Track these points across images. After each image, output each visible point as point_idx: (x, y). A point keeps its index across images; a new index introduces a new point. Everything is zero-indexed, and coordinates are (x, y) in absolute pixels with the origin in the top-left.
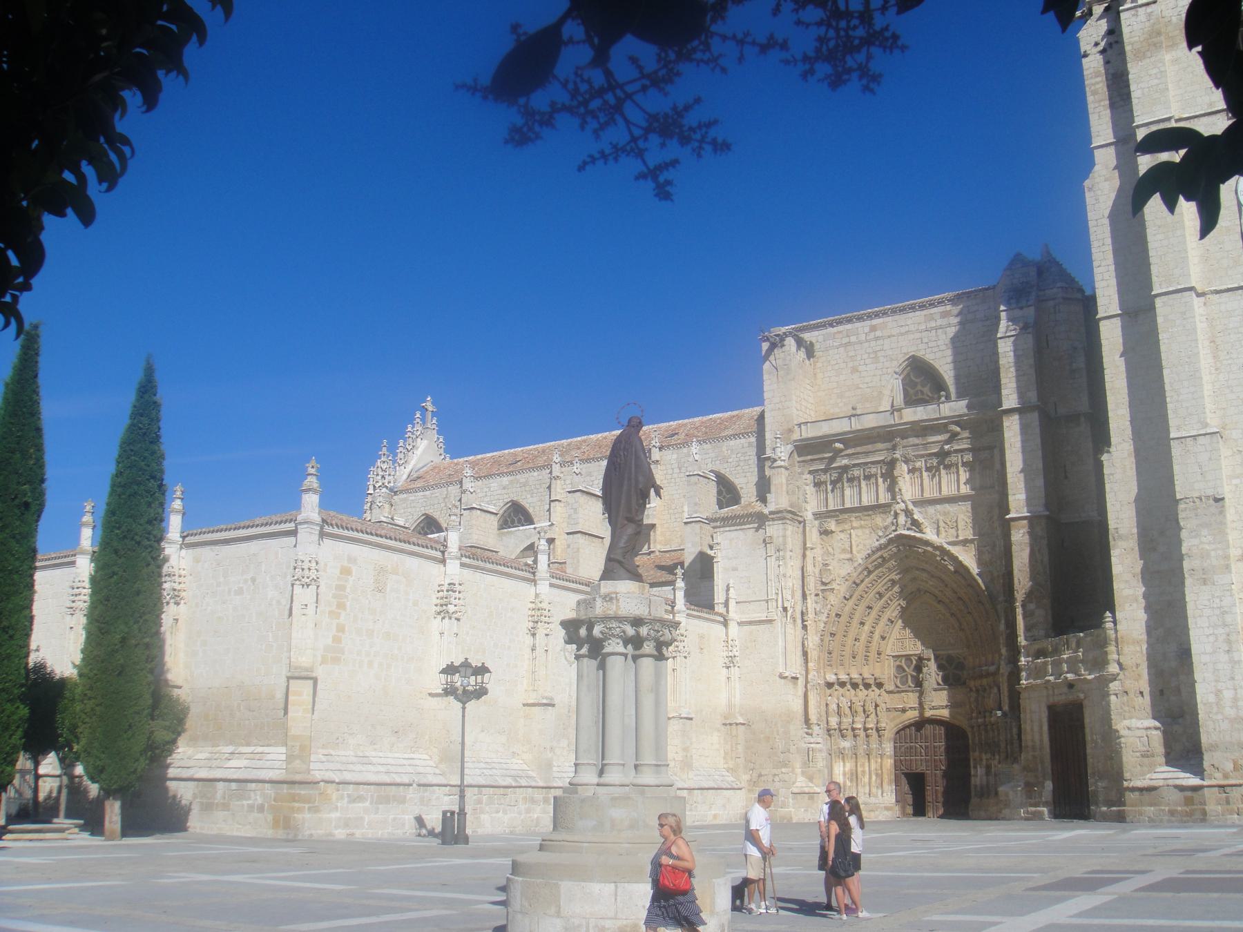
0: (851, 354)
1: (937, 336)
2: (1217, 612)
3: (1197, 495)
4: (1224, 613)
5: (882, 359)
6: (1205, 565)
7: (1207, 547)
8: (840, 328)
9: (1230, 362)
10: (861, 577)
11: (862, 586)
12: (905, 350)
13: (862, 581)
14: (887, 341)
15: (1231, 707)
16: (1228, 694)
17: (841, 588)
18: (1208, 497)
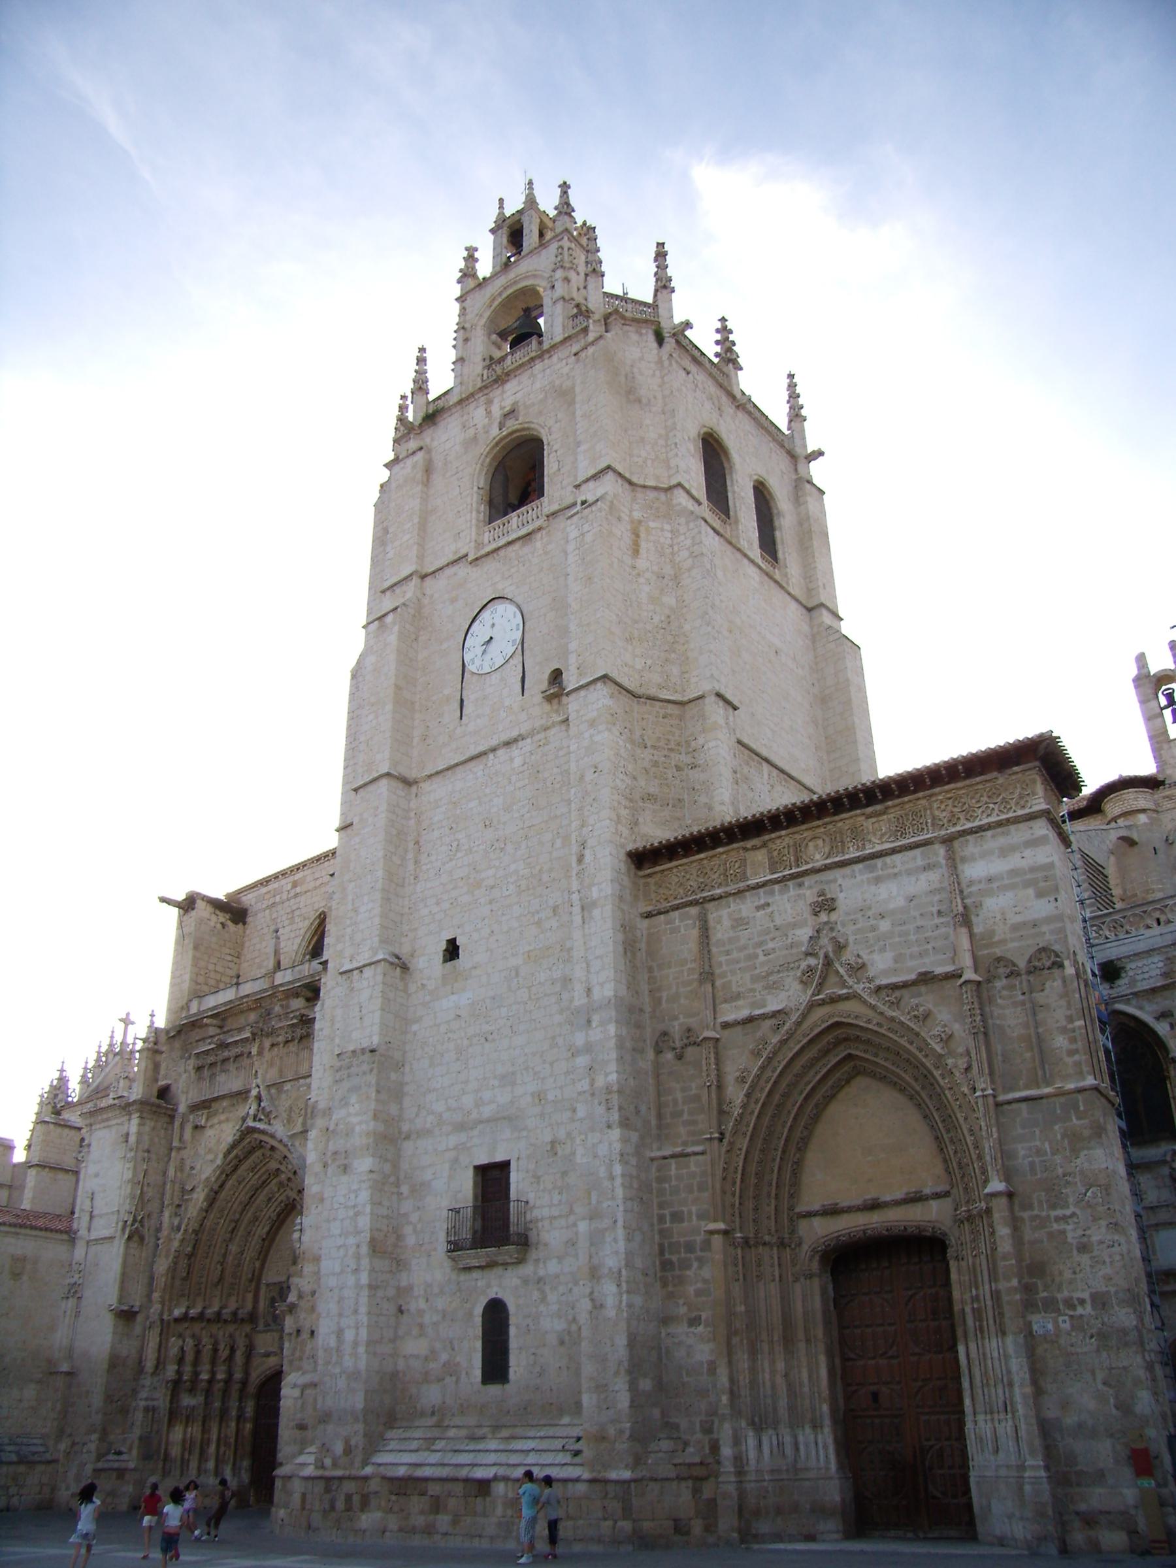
2: (351, 1213)
3: (352, 1048)
5: (297, 919)
7: (354, 1120)
8: (270, 888)
9: (429, 866)
10: (219, 1183)
11: (223, 1195)
12: (316, 906)
13: (222, 1186)
14: (303, 898)
16: (349, 1335)
17: (199, 1197)
18: (363, 1051)
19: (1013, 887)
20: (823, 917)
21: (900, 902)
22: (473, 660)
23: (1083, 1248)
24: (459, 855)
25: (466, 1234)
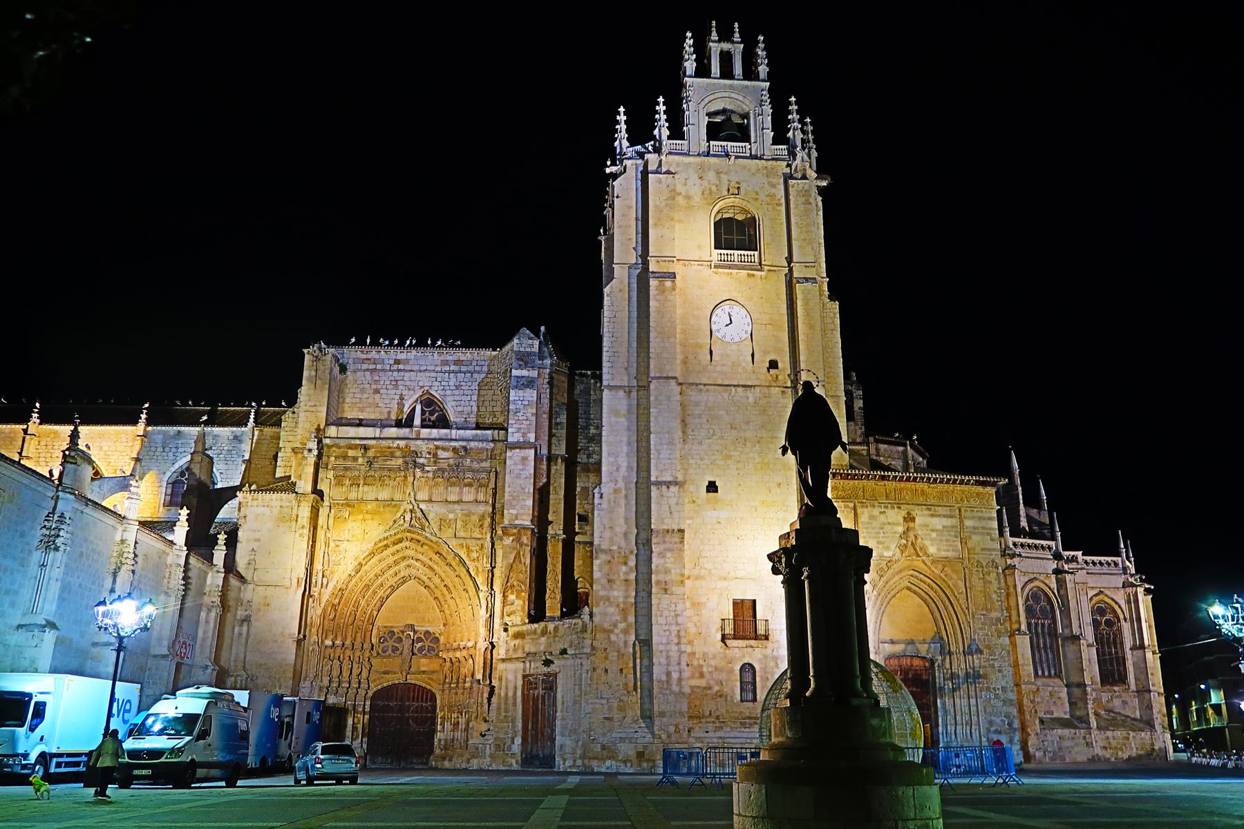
0: (377, 378)
1: (449, 378)
2: (673, 614)
3: (665, 527)
4: (677, 616)
5: (401, 387)
6: (667, 579)
7: (669, 565)
14: (407, 374)
15: (677, 685)
16: (675, 676)
19: (983, 534)
20: (911, 525)
21: (940, 527)
22: (718, 331)
23: (1000, 671)
24: (714, 437)
25: (729, 630)
